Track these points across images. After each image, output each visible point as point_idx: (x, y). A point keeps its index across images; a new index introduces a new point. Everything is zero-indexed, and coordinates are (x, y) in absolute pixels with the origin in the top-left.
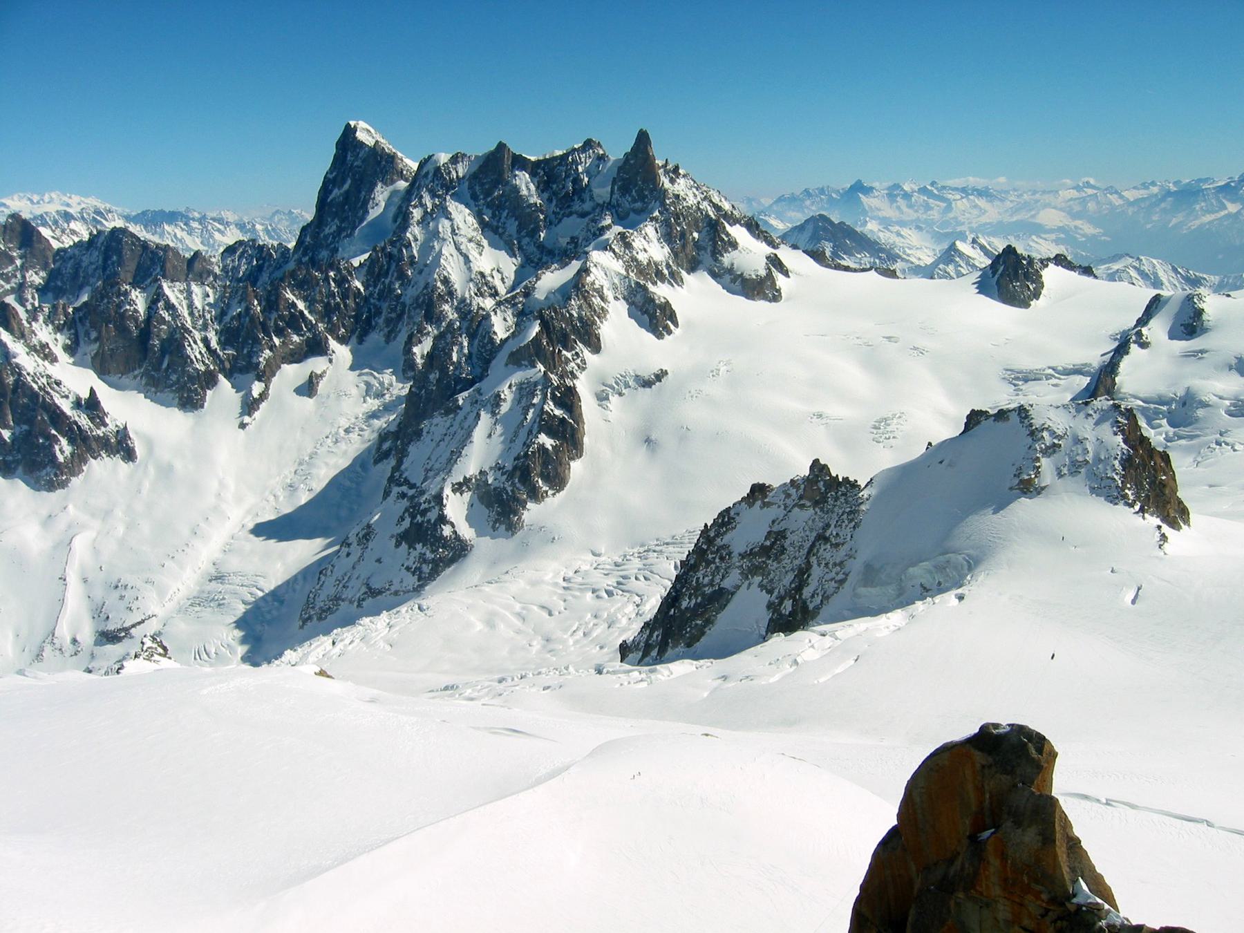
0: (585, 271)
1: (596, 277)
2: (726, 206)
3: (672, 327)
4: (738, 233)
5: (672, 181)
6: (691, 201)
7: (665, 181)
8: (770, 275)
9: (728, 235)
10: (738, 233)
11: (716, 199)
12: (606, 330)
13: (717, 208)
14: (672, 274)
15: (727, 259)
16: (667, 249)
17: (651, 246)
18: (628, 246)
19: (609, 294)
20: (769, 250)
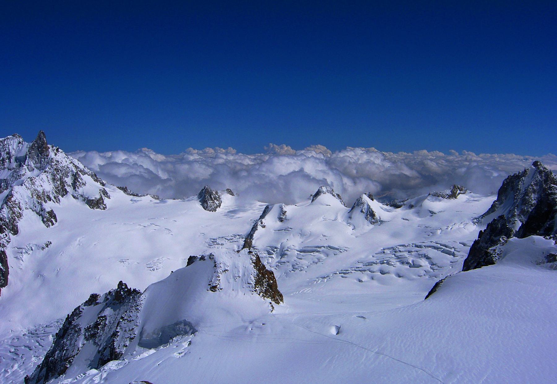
0: (10, 195)
1: (16, 197)
2: (81, 166)
3: (54, 222)
4: (86, 178)
5: (56, 155)
6: (64, 164)
7: (52, 155)
8: (101, 198)
9: (81, 179)
10: (86, 178)
11: (76, 164)
12: (21, 224)
13: (76, 167)
14: (55, 198)
15: (80, 190)
16: (52, 186)
17: (45, 184)
18: (33, 184)
19: (23, 206)
20: (101, 187)
